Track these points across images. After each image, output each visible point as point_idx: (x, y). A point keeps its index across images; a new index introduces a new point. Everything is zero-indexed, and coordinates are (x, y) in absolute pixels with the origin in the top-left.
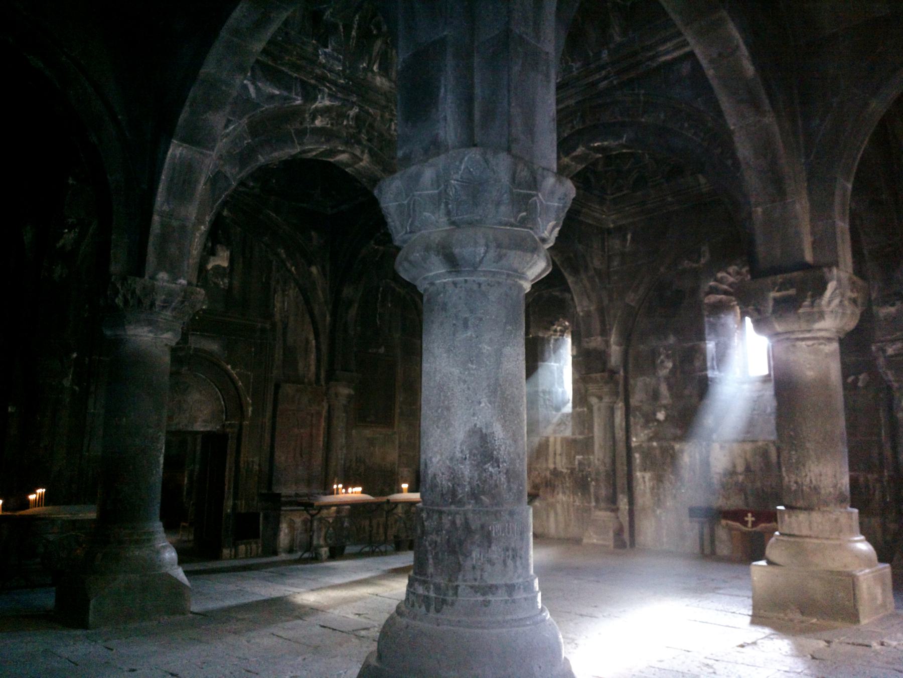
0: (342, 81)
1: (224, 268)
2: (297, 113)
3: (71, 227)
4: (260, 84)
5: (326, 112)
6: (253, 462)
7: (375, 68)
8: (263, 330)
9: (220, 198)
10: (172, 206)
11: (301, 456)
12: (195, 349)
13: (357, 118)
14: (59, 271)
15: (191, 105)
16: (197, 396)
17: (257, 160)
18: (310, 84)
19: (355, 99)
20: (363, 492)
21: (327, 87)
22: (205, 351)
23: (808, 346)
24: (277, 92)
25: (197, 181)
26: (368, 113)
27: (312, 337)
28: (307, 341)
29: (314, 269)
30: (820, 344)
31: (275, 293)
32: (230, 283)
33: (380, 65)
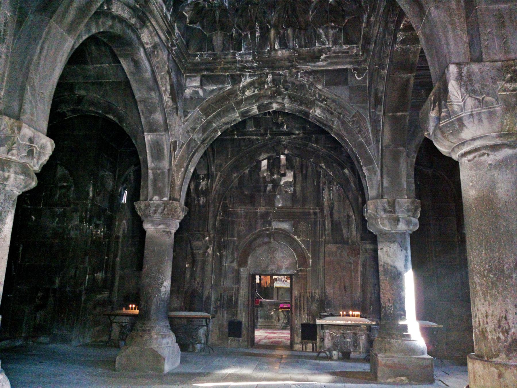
0: (255, 64)
1: (291, 182)
2: (232, 93)
3: (203, 179)
4: (205, 87)
5: (250, 86)
6: (315, 293)
7: (276, 47)
8: (315, 213)
9: (192, 151)
10: (156, 164)
11: (345, 290)
12: (276, 229)
13: (274, 80)
14: (202, 200)
15: (143, 114)
16: (281, 255)
17: (213, 126)
18: (237, 75)
19: (267, 71)
20: (361, 316)
21: (247, 72)
22: (281, 230)
23: (469, 161)
24: (215, 87)
25: (163, 149)
26: (280, 75)
27: (351, 213)
28: (349, 216)
29: (346, 171)
30: (483, 154)
31: (323, 190)
32: (295, 190)
33: (280, 44)
